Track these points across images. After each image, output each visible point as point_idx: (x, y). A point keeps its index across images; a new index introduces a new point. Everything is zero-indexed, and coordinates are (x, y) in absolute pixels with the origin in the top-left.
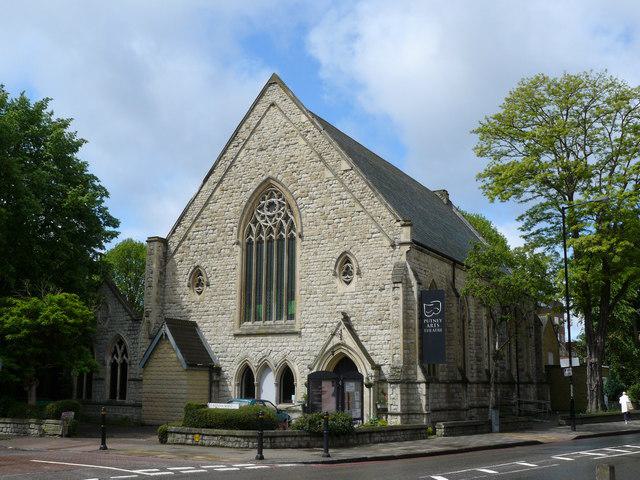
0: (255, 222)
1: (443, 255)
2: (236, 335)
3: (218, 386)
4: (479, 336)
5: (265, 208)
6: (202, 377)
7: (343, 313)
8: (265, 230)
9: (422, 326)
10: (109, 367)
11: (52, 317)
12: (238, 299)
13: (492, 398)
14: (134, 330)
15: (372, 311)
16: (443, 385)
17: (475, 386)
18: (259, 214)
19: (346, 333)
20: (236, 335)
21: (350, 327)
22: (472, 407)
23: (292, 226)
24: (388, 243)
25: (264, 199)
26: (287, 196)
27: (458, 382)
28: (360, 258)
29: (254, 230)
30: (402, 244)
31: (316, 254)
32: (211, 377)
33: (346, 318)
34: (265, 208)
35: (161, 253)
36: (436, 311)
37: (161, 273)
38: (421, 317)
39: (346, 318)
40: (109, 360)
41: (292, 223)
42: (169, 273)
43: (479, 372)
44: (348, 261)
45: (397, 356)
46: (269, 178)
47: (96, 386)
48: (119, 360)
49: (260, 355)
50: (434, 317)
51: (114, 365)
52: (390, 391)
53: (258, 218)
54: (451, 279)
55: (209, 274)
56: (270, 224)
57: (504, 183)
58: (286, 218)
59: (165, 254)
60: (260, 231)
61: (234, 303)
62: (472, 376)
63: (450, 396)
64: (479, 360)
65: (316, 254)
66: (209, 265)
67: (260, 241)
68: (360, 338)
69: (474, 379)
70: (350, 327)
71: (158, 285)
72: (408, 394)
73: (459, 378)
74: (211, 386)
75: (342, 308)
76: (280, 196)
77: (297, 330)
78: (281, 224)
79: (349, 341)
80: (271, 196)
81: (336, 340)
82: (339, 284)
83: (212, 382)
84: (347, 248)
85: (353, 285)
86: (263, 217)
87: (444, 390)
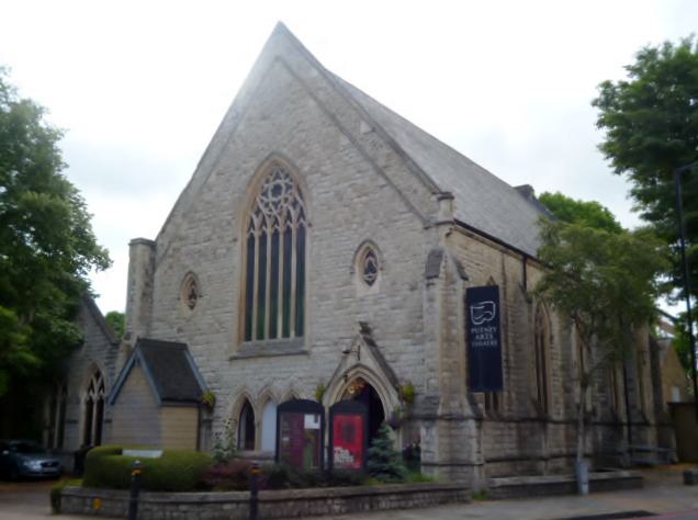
0: (258, 212)
1: (508, 247)
2: (233, 359)
3: (210, 427)
4: (566, 358)
5: (270, 194)
6: (188, 416)
7: (362, 324)
8: (268, 221)
9: (470, 337)
10: (83, 407)
11: (69, 330)
12: (236, 312)
13: (585, 444)
14: (112, 357)
15: (401, 319)
16: (513, 425)
17: (563, 426)
18: (262, 201)
19: (365, 350)
20: (233, 359)
21: (371, 343)
22: (555, 456)
23: (302, 215)
24: (419, 226)
25: (267, 181)
26: (294, 174)
27: (533, 420)
28: (387, 250)
29: (257, 222)
30: (439, 224)
31: (329, 246)
32: (200, 416)
33: (366, 329)
34: (270, 194)
35: (147, 259)
36: (488, 316)
37: (147, 285)
38: (469, 325)
39: (366, 329)
40: (84, 396)
41: (302, 209)
42: (140, 282)
43: (567, 407)
44: (371, 254)
45: (432, 381)
46: (272, 154)
47: (68, 430)
48: (95, 397)
49: (261, 385)
50: (485, 325)
51: (90, 403)
52: (423, 432)
53: (261, 207)
54: (520, 279)
55: (206, 289)
56: (275, 212)
57: (612, 127)
58: (295, 204)
59: (152, 260)
60: (264, 223)
61: (231, 316)
62: (557, 411)
63: (521, 441)
64: (567, 390)
65: (329, 246)
66: (205, 270)
67: (288, 231)
68: (387, 357)
69: (561, 418)
70: (371, 343)
71: (142, 299)
72: (451, 436)
73: (533, 414)
74: (199, 426)
75: (362, 318)
76: (287, 176)
77: (306, 348)
78: (289, 212)
79: (368, 360)
80: (277, 177)
81: (352, 360)
82: (407, 287)
83: (200, 423)
84: (368, 235)
85: (376, 287)
86: (267, 205)
87: (514, 432)
